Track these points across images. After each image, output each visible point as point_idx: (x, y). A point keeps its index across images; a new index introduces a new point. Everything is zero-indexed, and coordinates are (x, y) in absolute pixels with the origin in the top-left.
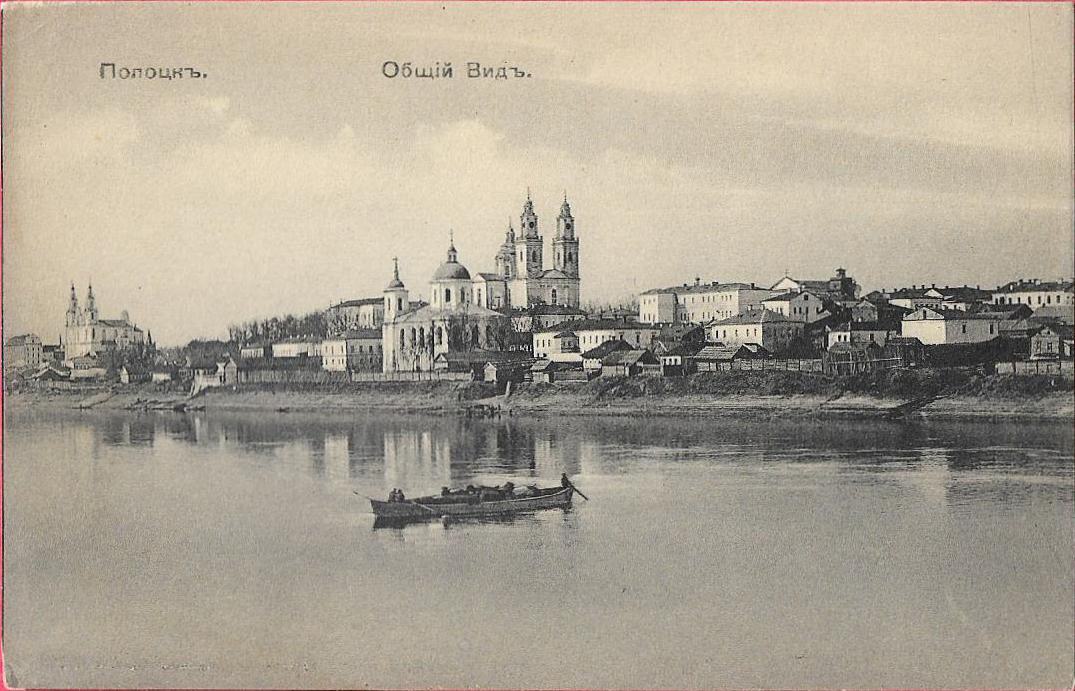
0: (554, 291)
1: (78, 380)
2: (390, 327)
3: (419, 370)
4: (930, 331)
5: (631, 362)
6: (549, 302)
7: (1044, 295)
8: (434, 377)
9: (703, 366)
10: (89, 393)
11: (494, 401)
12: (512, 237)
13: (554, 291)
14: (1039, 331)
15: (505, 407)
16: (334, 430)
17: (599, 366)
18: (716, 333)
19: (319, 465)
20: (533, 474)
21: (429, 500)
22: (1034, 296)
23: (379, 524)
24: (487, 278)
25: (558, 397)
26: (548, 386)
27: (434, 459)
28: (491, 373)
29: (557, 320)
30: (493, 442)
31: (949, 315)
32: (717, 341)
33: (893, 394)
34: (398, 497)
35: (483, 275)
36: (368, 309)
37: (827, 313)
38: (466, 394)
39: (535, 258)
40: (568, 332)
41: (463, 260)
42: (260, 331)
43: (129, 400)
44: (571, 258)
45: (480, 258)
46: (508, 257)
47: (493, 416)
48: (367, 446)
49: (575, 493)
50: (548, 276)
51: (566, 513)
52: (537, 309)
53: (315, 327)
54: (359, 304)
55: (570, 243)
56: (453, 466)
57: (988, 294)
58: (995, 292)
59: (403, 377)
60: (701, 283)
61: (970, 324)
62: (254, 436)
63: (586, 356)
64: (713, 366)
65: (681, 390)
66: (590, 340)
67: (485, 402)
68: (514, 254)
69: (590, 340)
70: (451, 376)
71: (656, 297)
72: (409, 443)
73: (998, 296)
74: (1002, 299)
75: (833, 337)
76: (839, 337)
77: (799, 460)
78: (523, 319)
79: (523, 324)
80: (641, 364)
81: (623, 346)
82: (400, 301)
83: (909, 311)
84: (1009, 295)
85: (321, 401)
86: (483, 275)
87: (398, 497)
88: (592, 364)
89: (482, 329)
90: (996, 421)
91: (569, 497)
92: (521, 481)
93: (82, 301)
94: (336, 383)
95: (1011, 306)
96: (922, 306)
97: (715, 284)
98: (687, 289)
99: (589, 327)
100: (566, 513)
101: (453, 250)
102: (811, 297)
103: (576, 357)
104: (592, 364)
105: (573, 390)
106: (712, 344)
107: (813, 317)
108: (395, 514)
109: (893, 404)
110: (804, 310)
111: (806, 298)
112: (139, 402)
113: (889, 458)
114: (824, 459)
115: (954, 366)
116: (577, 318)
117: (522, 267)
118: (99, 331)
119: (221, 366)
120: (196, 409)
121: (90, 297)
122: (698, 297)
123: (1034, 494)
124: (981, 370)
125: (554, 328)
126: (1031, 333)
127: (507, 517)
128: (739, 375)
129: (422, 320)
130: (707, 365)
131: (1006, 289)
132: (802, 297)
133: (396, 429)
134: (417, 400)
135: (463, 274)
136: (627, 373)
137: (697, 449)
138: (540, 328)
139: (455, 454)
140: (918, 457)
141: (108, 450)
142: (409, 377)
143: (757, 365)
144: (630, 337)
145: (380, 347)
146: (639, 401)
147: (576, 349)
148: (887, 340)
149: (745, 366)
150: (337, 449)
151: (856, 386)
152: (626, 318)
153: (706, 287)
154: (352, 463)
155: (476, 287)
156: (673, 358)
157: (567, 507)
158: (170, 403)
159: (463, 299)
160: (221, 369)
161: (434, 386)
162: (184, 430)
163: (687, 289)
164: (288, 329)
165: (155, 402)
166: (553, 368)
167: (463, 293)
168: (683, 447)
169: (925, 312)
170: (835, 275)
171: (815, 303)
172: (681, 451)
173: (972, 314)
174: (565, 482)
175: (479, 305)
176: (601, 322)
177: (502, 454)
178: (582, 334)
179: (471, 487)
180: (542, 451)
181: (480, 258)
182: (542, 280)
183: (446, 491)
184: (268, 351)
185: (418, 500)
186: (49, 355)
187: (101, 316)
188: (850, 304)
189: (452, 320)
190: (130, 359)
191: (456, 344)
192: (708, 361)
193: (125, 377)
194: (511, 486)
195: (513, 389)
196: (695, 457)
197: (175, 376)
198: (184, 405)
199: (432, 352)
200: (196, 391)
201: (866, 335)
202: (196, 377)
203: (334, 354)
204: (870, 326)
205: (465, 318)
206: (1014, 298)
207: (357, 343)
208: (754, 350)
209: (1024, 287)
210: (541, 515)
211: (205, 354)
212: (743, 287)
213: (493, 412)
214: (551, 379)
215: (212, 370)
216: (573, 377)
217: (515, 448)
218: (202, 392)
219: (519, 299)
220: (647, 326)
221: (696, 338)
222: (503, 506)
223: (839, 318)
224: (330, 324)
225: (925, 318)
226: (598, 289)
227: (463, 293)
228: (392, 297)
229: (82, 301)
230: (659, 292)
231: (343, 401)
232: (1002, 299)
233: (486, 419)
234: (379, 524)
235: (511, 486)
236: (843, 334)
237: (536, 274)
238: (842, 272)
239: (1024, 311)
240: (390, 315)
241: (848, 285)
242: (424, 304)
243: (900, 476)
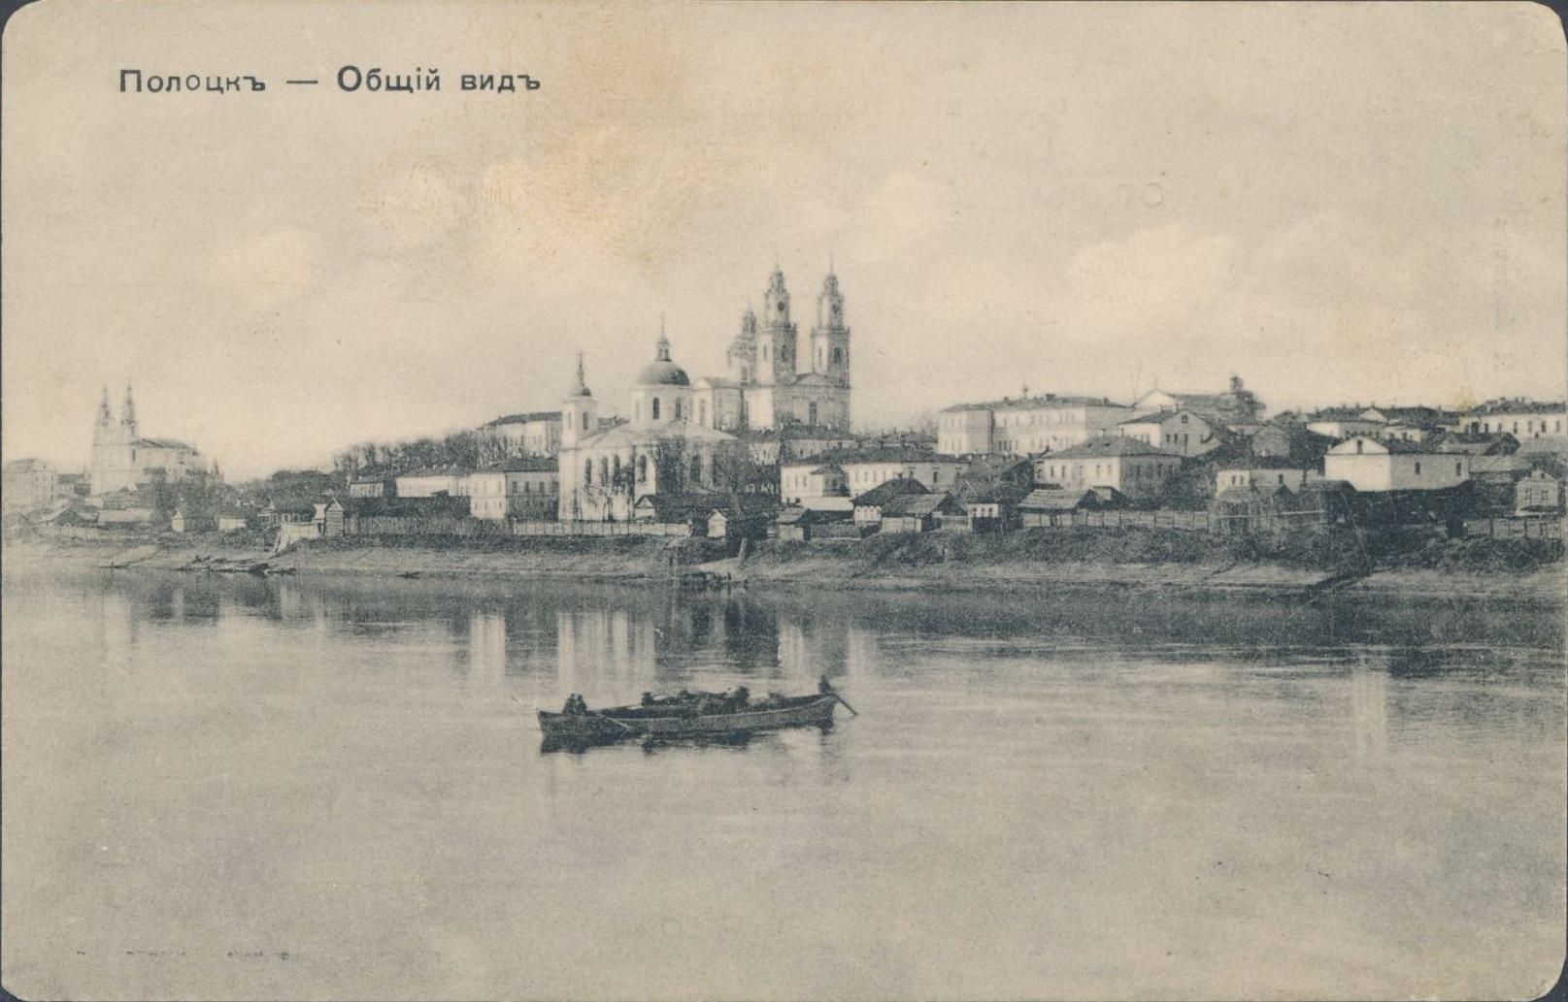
1: (108, 526)
3: (611, 520)
4: (1366, 470)
5: (926, 511)
6: (806, 420)
7: (1536, 419)
8: (634, 530)
9: (1031, 520)
10: (128, 544)
11: (722, 567)
12: (751, 325)
13: (813, 405)
14: (1528, 473)
15: (738, 576)
16: (486, 606)
17: (877, 518)
18: (1051, 470)
19: (462, 657)
20: (776, 676)
21: (623, 712)
22: (1522, 420)
23: (548, 747)
24: (716, 385)
25: (815, 564)
26: (802, 545)
27: (631, 649)
28: (718, 525)
29: (814, 446)
30: (718, 628)
31: (1394, 448)
32: (1049, 480)
33: (1310, 564)
34: (575, 706)
35: (707, 380)
36: (536, 429)
37: (1215, 443)
38: (683, 554)
39: (786, 353)
40: (832, 463)
41: (680, 359)
42: (380, 458)
43: (182, 558)
44: (838, 356)
45: (707, 357)
46: (745, 348)
47: (718, 589)
48: (532, 625)
49: (839, 706)
50: (804, 382)
51: (825, 733)
52: (788, 430)
53: (461, 453)
54: (520, 419)
55: (839, 333)
56: (659, 661)
57: (1453, 417)
58: (1463, 415)
59: (588, 530)
60: (1030, 395)
61: (1424, 459)
62: (364, 617)
63: (856, 503)
64: (1046, 520)
65: (998, 556)
66: (864, 478)
67: (703, 568)
68: (754, 348)
69: (864, 478)
70: (658, 529)
71: (964, 416)
72: (595, 625)
73: (1465, 422)
74: (1475, 425)
75: (1227, 480)
76: (1234, 479)
77: (1173, 659)
78: (768, 446)
79: (765, 453)
80: (938, 515)
81: (912, 487)
82: (585, 417)
83: (1336, 442)
84: (1484, 420)
85: (467, 562)
86: (707, 380)
87: (575, 706)
88: (866, 515)
89: (706, 461)
90: (1468, 605)
91: (830, 708)
92: (760, 690)
94: (492, 538)
95: (1486, 437)
96: (1354, 435)
97: (1050, 397)
98: (1009, 403)
99: (864, 459)
100: (825, 733)
102: (1191, 418)
103: (843, 504)
104: (866, 515)
105: (839, 551)
106: (1044, 486)
107: (1196, 449)
108: (575, 731)
109: (1316, 577)
110: (1181, 438)
111: (1185, 419)
112: (198, 560)
113: (1308, 658)
114: (1208, 658)
115: (1389, 525)
116: (846, 444)
117: (765, 371)
119: (320, 508)
120: (283, 572)
121: (130, 402)
122: (1024, 416)
123: (1519, 715)
124: (1441, 529)
125: (813, 460)
126: (1517, 475)
127: (739, 739)
128: (1084, 535)
129: (614, 449)
130: (1037, 517)
131: (1480, 410)
132: (1177, 419)
133: (576, 607)
134: (609, 564)
135: (679, 379)
136: (919, 528)
137: (1023, 642)
138: (788, 458)
139: (662, 645)
140: (1348, 660)
141: (149, 632)
142: (596, 529)
143: (1112, 518)
144: (923, 473)
145: (556, 484)
146: (936, 570)
147: (844, 492)
148: (1304, 485)
149: (1093, 519)
150: (489, 635)
151: (1253, 550)
152: (917, 446)
153: (1038, 403)
154: (511, 654)
156: (987, 507)
157: (826, 725)
158: (243, 562)
159: (678, 415)
161: (629, 544)
162: (260, 600)
164: (421, 456)
165: (221, 561)
166: (810, 520)
167: (678, 406)
168: (1000, 637)
169: (1360, 443)
170: (1225, 386)
171: (1197, 429)
172: (995, 643)
173: (1429, 448)
174: (825, 686)
175: (702, 423)
176: (881, 450)
177: (733, 646)
179: (685, 692)
180: (791, 645)
181: (707, 357)
182: (796, 389)
183: (648, 699)
184: (390, 485)
185: (606, 712)
187: (146, 431)
188: (1249, 430)
189: (664, 444)
190: (184, 496)
191: (668, 476)
192: (1040, 511)
193: (178, 524)
194: (743, 693)
195: (750, 549)
196: (1016, 653)
197: (253, 522)
198: (266, 566)
199: (632, 493)
200: (283, 546)
201: (1270, 477)
202: (284, 526)
203: (488, 495)
204: (1272, 462)
205: (680, 443)
206: (1493, 423)
207: (523, 479)
209: (1505, 407)
210: (789, 737)
211: (297, 491)
212: (1092, 403)
213: (719, 583)
214: (807, 536)
215: (308, 515)
216: (837, 534)
217: (751, 634)
218: (292, 548)
219: (762, 413)
220: (947, 459)
221: (1023, 473)
222: (727, 725)
223: (1232, 450)
224: (481, 449)
225: (1360, 452)
226: (878, 404)
227: (678, 406)
228: (571, 411)
229: (118, 413)
230: (967, 408)
231: (496, 564)
232: (1475, 425)
233: (709, 594)
234: (548, 747)
235: (743, 693)
236: (1238, 473)
237: (788, 381)
238: (1235, 380)
239: (1508, 444)
240: (569, 437)
241: (1248, 403)
242: (618, 422)
243: (1319, 685)
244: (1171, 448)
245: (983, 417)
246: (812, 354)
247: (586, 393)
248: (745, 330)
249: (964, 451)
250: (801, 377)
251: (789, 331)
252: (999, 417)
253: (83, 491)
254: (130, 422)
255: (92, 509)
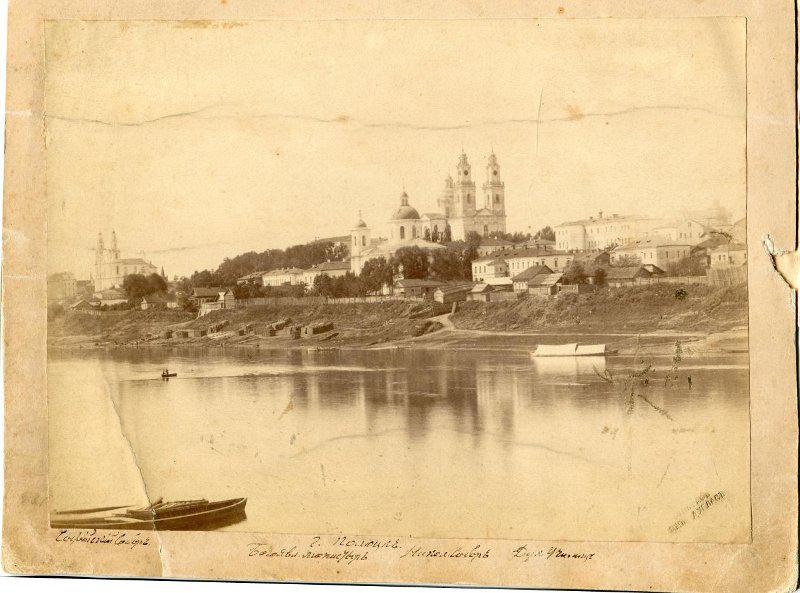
0: (486, 226)
2: (357, 259)
5: (553, 283)
12: (450, 183)
13: (486, 226)
24: (433, 217)
29: (490, 250)
35: (427, 215)
37: (707, 237)
39: (469, 199)
40: (500, 257)
41: (413, 204)
44: (498, 199)
45: (428, 203)
46: (448, 201)
50: (482, 214)
55: (497, 185)
63: (516, 280)
66: (519, 266)
93: (108, 245)
97: (615, 216)
98: (593, 220)
101: (406, 195)
103: (507, 281)
110: (688, 234)
117: (459, 207)
118: (122, 267)
119: (222, 294)
125: (487, 257)
135: (413, 215)
144: (549, 262)
147: (507, 274)
155: (424, 225)
160: (222, 298)
163: (593, 220)
178: (510, 262)
186: (83, 288)
187: (123, 256)
200: (202, 315)
202: (203, 305)
208: (650, 269)
211: (207, 281)
229: (108, 245)
230: (570, 224)
237: (471, 214)
244: (683, 241)
245: (579, 230)
246: (482, 200)
247: (363, 225)
248: (447, 186)
249: (570, 248)
250: (478, 212)
251: (469, 185)
252: (588, 229)
253: (92, 289)
254: (116, 252)
255: (97, 300)
